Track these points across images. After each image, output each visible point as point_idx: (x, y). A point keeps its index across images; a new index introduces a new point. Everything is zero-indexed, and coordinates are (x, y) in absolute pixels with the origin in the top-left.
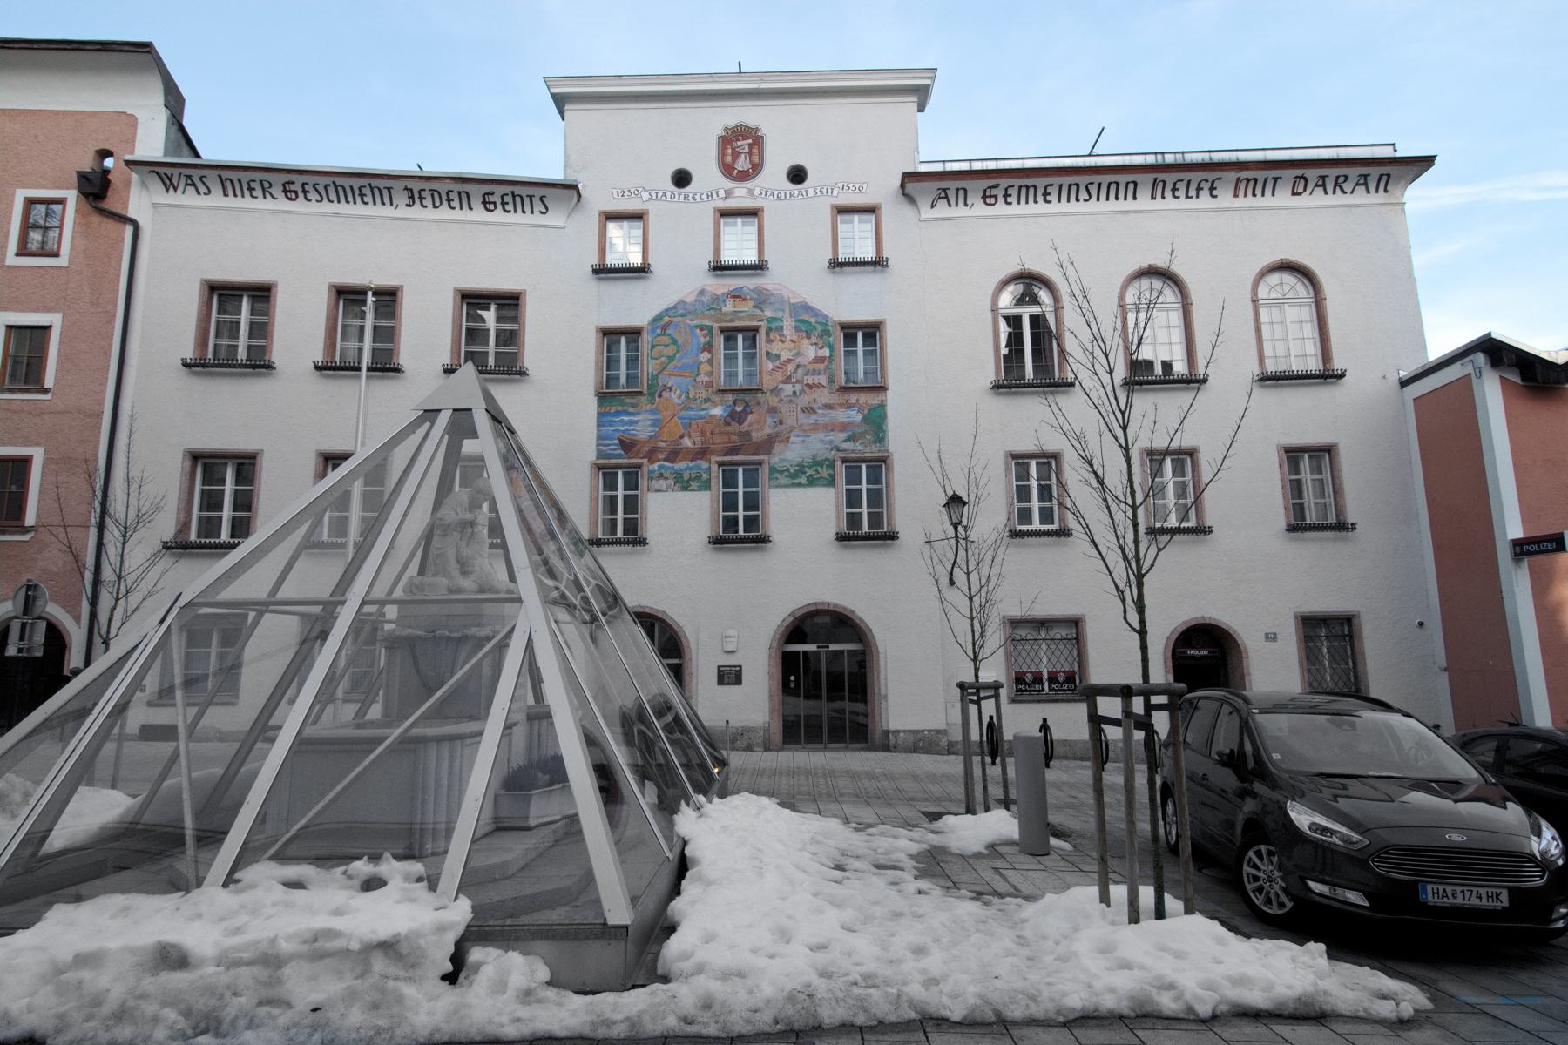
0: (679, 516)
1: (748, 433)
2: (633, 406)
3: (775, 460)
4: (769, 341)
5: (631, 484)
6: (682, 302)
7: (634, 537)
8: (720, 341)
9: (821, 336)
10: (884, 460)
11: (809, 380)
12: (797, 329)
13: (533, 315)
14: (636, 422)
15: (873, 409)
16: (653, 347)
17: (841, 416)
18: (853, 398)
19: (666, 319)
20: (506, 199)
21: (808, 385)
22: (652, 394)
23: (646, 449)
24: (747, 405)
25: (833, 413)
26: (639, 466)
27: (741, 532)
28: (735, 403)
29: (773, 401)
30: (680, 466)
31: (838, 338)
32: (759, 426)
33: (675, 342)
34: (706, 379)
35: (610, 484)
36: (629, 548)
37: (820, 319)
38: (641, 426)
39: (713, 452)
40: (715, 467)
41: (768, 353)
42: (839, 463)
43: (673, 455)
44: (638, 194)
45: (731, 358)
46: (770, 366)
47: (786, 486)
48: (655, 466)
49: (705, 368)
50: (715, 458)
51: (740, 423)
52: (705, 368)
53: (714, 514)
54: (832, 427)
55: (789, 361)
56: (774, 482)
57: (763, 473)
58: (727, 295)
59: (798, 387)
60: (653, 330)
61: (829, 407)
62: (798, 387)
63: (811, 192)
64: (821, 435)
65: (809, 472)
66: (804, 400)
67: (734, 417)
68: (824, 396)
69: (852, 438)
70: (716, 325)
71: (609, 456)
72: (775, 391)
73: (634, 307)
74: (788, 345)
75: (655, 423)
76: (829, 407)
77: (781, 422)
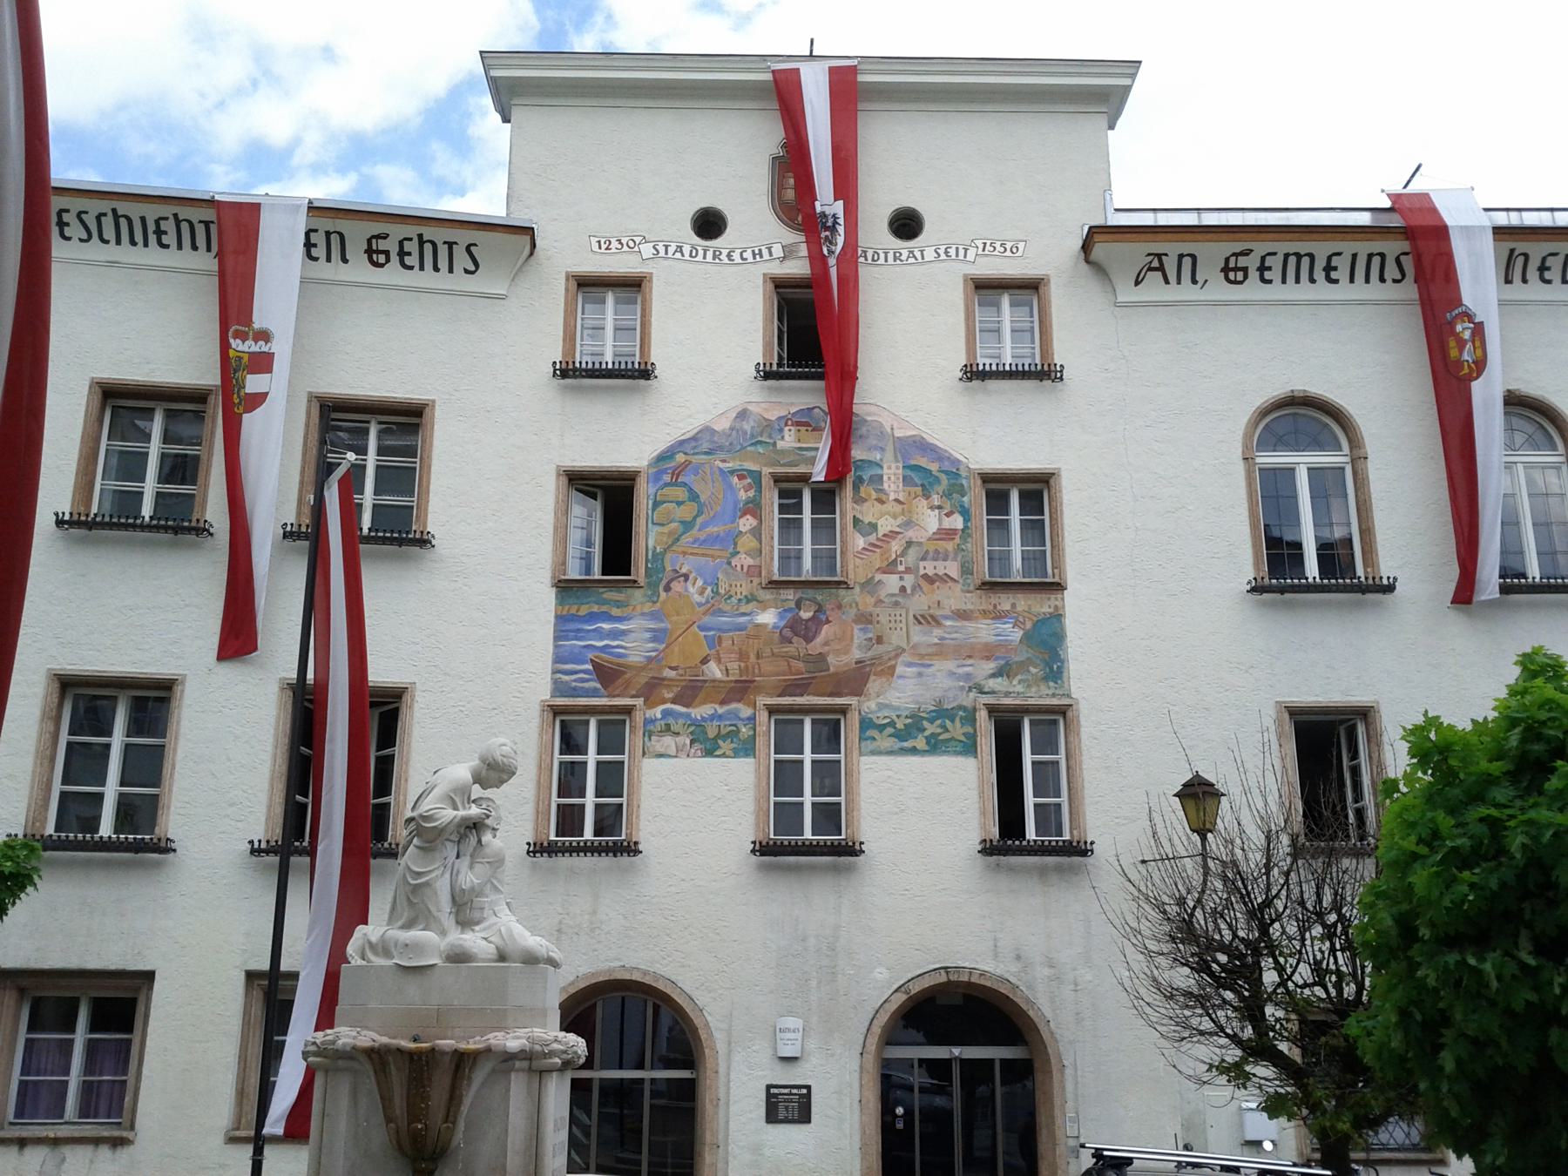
0: (697, 799)
1: (822, 658)
2: (619, 604)
3: (870, 705)
4: (859, 500)
5: (612, 740)
6: (707, 430)
7: (613, 840)
8: (771, 499)
9: (948, 495)
10: (1063, 711)
11: (929, 568)
12: (907, 481)
13: (446, 444)
14: (624, 633)
15: (1042, 622)
16: (656, 504)
17: (984, 631)
18: (1005, 601)
19: (680, 458)
20: (407, 246)
21: (925, 577)
22: (653, 586)
23: (643, 679)
24: (820, 609)
25: (970, 626)
26: (628, 710)
27: (808, 834)
28: (798, 605)
29: (866, 602)
30: (701, 711)
31: (976, 498)
32: (842, 645)
33: (694, 497)
34: (750, 561)
35: (571, 742)
36: (605, 861)
37: (947, 466)
38: (633, 639)
39: (760, 690)
40: (763, 716)
41: (856, 521)
42: (982, 715)
43: (690, 692)
44: (633, 247)
45: (790, 527)
46: (861, 542)
47: (890, 753)
48: (657, 712)
49: (747, 542)
50: (763, 700)
51: (808, 640)
52: (747, 542)
53: (761, 799)
54: (969, 652)
55: (892, 535)
56: (869, 745)
57: (850, 730)
58: (785, 420)
59: (909, 581)
60: (657, 477)
61: (963, 615)
62: (909, 581)
63: (930, 254)
64: (950, 665)
65: (931, 729)
66: (920, 603)
67: (799, 630)
68: (955, 598)
69: (1002, 672)
70: (766, 471)
71: (575, 692)
72: (870, 585)
73: (624, 438)
74: (891, 507)
75: (657, 635)
76: (963, 615)
77: (879, 640)
